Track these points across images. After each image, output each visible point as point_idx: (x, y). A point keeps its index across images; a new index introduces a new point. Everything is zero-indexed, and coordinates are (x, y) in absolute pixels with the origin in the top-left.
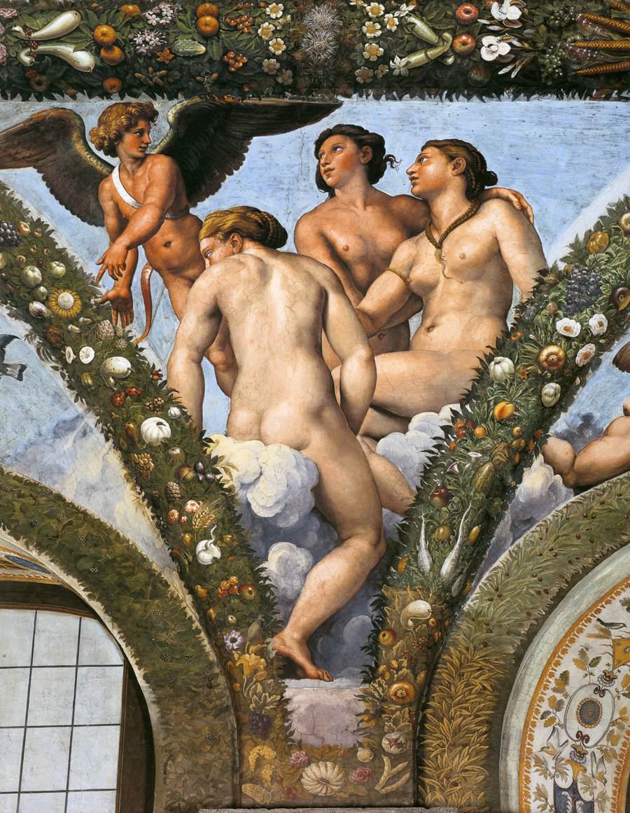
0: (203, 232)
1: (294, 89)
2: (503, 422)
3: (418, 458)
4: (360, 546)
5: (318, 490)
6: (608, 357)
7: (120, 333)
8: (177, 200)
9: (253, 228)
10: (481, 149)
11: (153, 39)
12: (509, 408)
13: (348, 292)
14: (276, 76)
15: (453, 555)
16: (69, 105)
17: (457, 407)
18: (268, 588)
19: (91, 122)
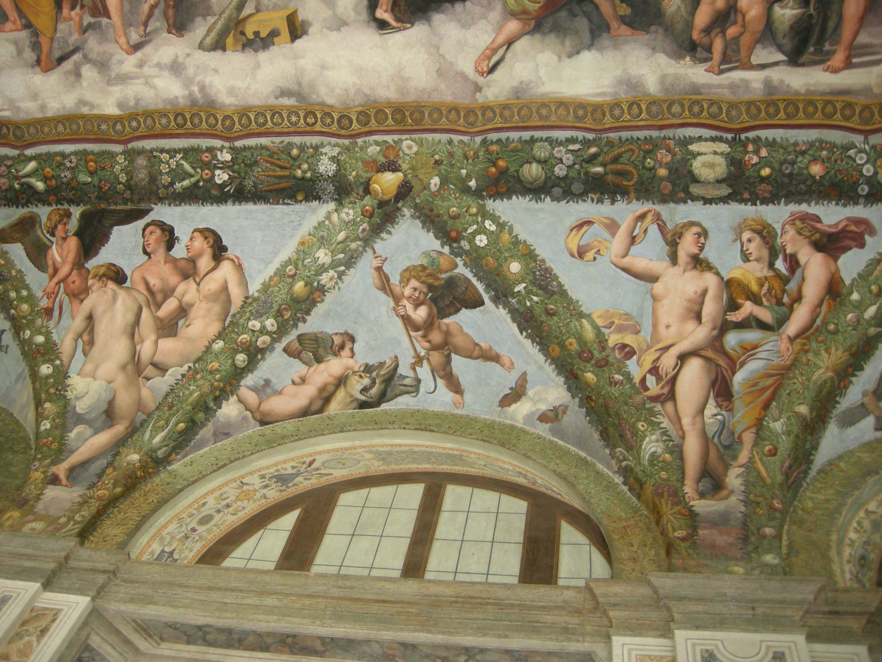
0: (90, 276)
1: (132, 200)
2: (211, 372)
3: (165, 388)
5: (111, 403)
6: (280, 347)
8: (80, 260)
9: (113, 274)
10: (220, 233)
13: (152, 307)
14: (123, 194)
15: (162, 434)
16: (34, 209)
17: (191, 365)
18: (65, 444)
19: (44, 219)
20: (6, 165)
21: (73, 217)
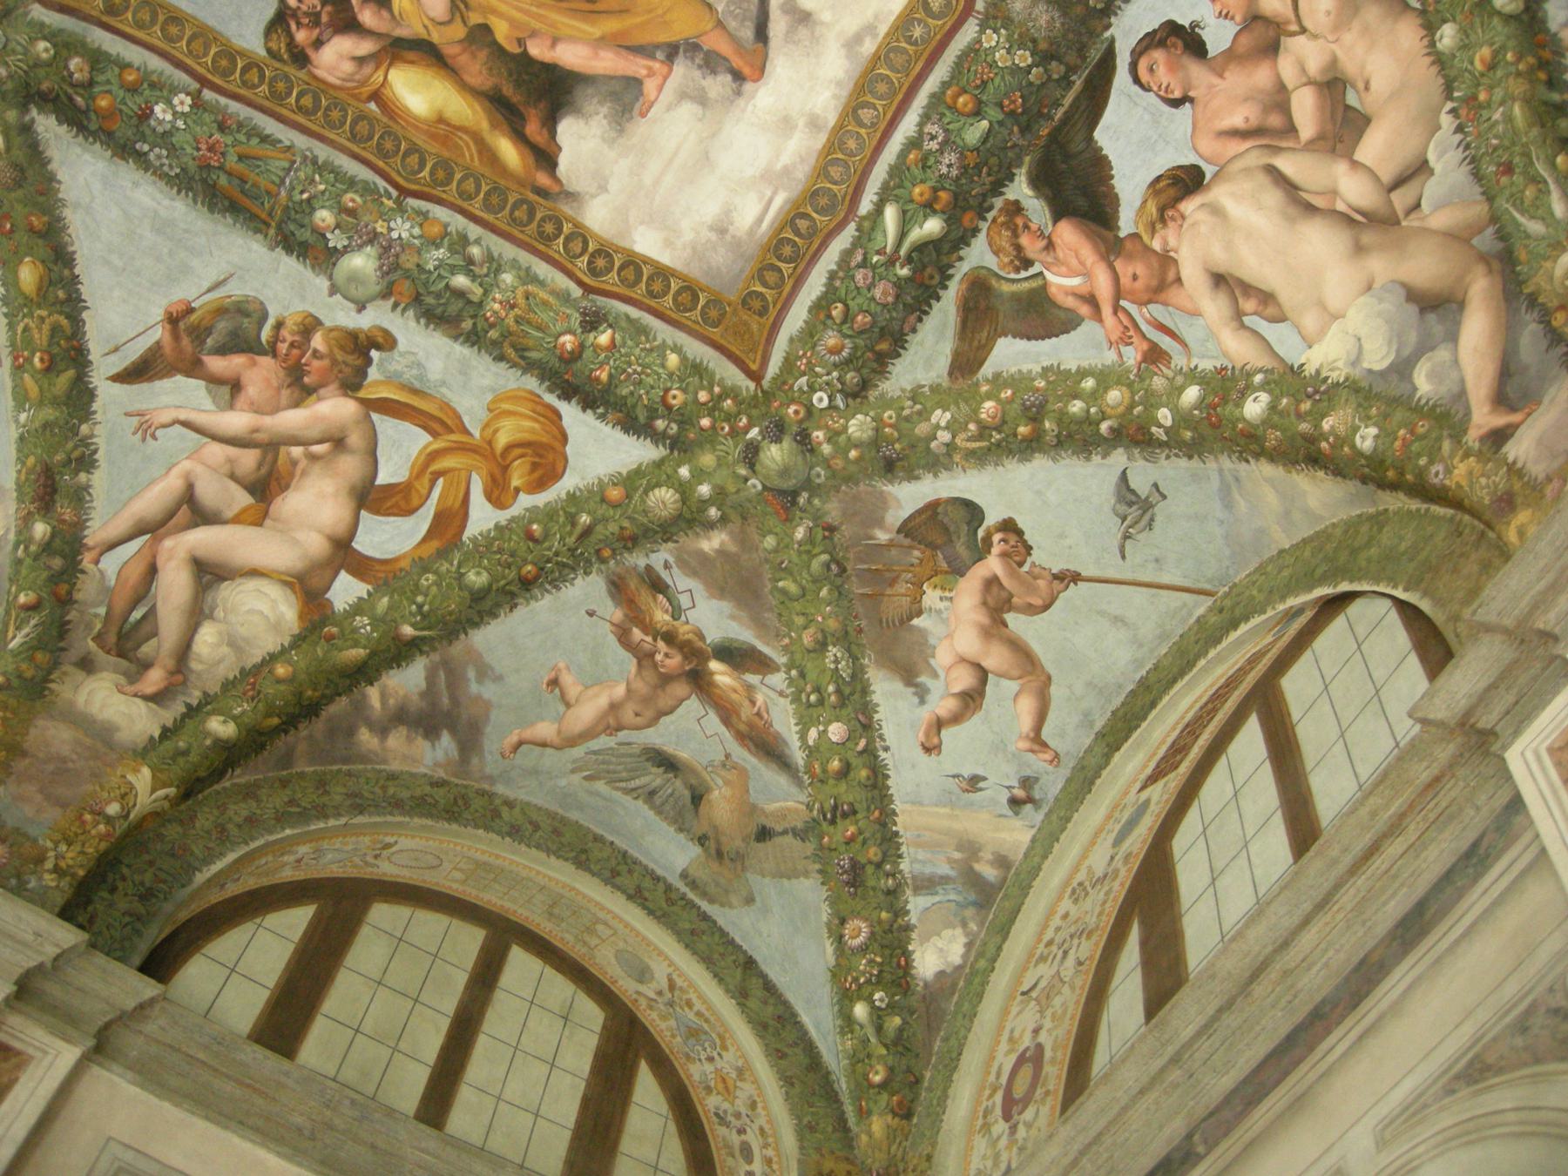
0: (1146, 238)
1: (1072, 69)
2: (1492, 67)
3: (1461, 175)
4: (1480, 290)
7: (1170, 374)
8: (1105, 240)
9: (1172, 192)
11: (950, 158)
12: (1485, 52)
13: (1284, 144)
14: (1050, 77)
16: (962, 269)
17: (1449, 105)
19: (991, 262)
20: (859, 266)
21: (1025, 203)
